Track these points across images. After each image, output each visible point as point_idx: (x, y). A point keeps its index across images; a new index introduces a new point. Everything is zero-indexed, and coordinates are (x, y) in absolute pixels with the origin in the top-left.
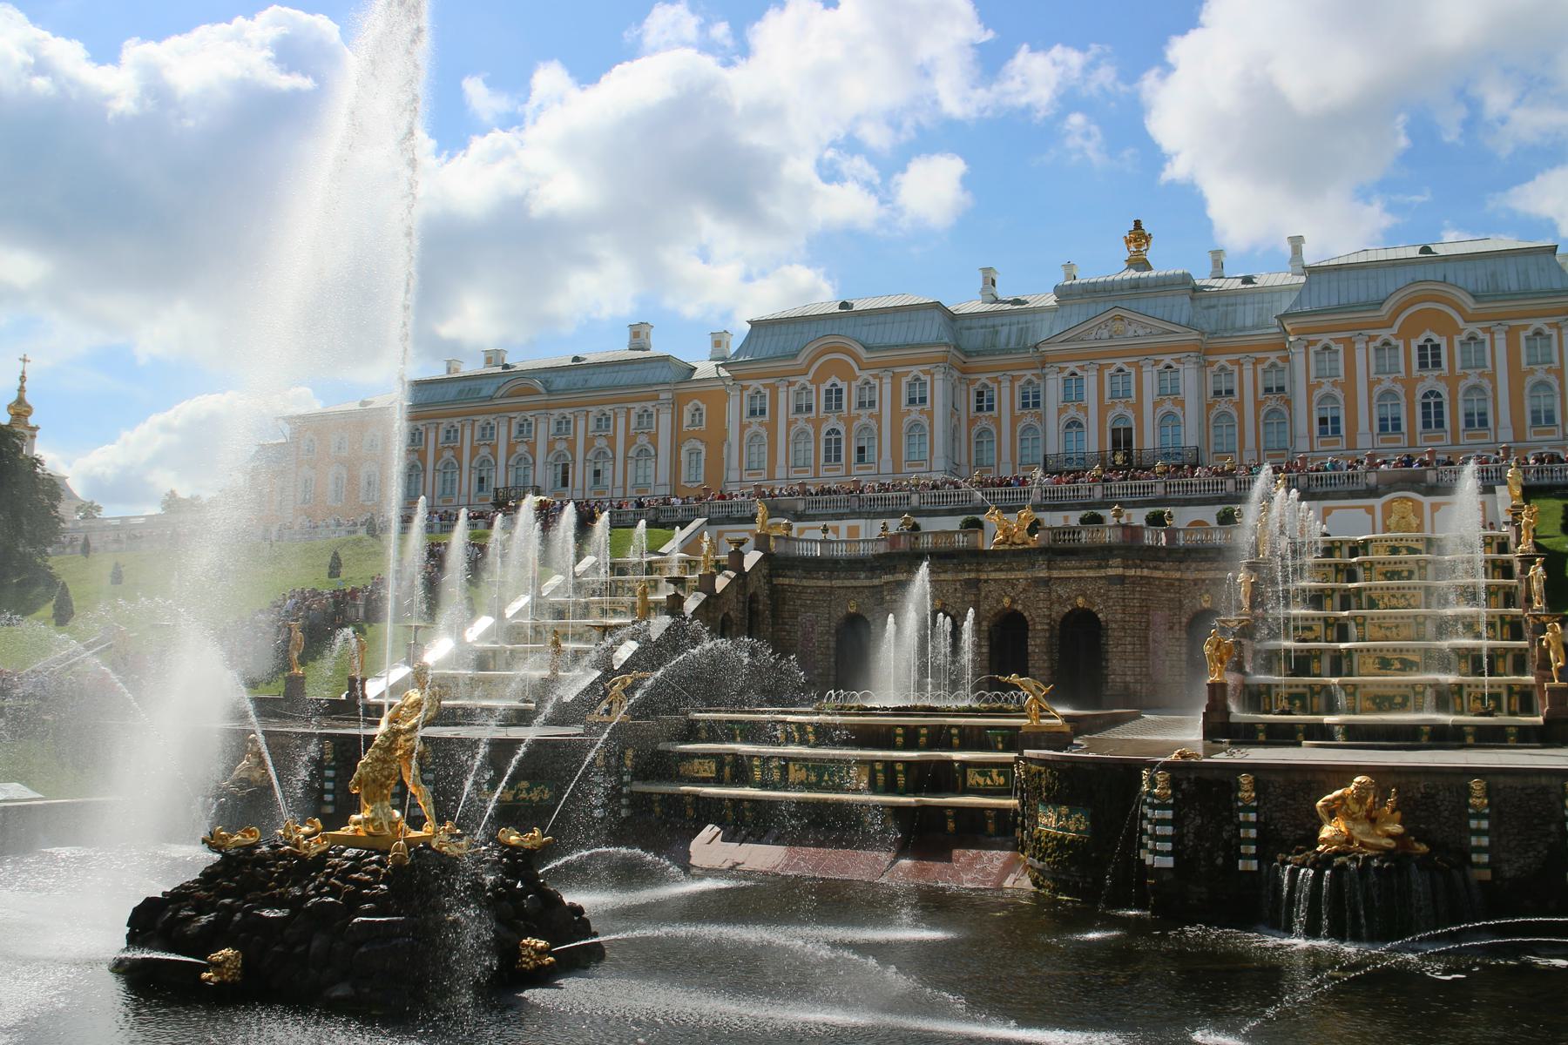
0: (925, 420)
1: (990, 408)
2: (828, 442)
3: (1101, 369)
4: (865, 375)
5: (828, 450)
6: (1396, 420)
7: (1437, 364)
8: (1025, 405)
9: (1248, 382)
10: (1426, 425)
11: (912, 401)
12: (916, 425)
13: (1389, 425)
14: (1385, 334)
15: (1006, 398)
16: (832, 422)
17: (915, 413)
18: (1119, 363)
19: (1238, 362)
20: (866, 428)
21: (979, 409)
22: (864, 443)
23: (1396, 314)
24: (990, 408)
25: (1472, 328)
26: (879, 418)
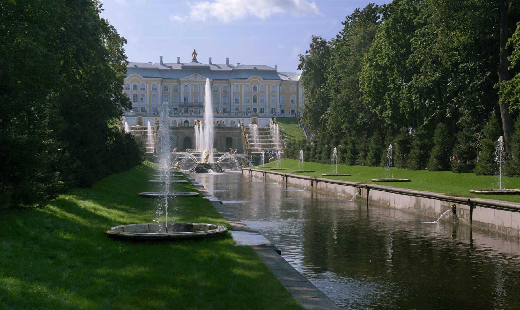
0: (156, 94)
1: (167, 90)
2: (134, 97)
3: (192, 85)
4: (143, 83)
5: (134, 99)
6: (249, 100)
7: (256, 90)
8: (174, 91)
9: (220, 90)
10: (254, 102)
11: (153, 89)
12: (154, 95)
13: (247, 101)
14: (248, 84)
15: (171, 89)
16: (135, 92)
17: (154, 92)
18: (196, 84)
19: (219, 86)
20: (143, 95)
21: (164, 90)
22: (142, 97)
23: (250, 80)
24: (167, 90)
25: (263, 84)
26: (146, 93)
